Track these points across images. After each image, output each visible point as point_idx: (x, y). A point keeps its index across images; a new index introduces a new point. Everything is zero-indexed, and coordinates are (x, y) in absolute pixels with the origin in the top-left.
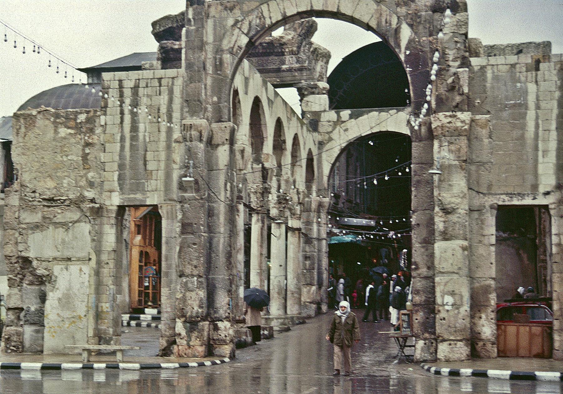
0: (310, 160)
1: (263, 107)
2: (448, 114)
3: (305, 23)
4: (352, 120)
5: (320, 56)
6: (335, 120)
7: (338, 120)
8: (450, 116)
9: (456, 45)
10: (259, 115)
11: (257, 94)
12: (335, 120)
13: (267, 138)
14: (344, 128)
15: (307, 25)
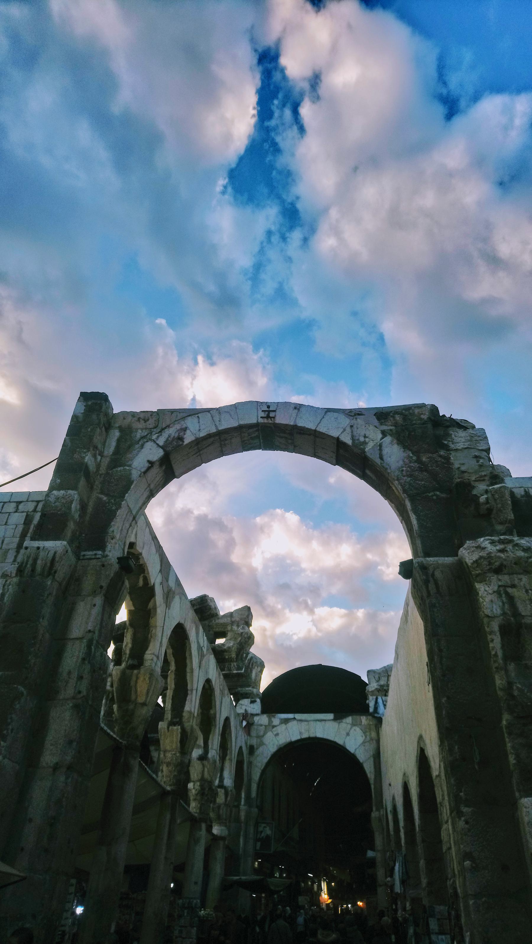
0: (240, 764)
1: (190, 647)
2: (496, 538)
3: (243, 634)
4: (283, 725)
5: (254, 664)
6: (267, 724)
7: (269, 725)
8: (501, 542)
9: (478, 462)
10: (185, 659)
11: (182, 622)
12: (267, 724)
13: (192, 690)
14: (275, 733)
15: (246, 636)
